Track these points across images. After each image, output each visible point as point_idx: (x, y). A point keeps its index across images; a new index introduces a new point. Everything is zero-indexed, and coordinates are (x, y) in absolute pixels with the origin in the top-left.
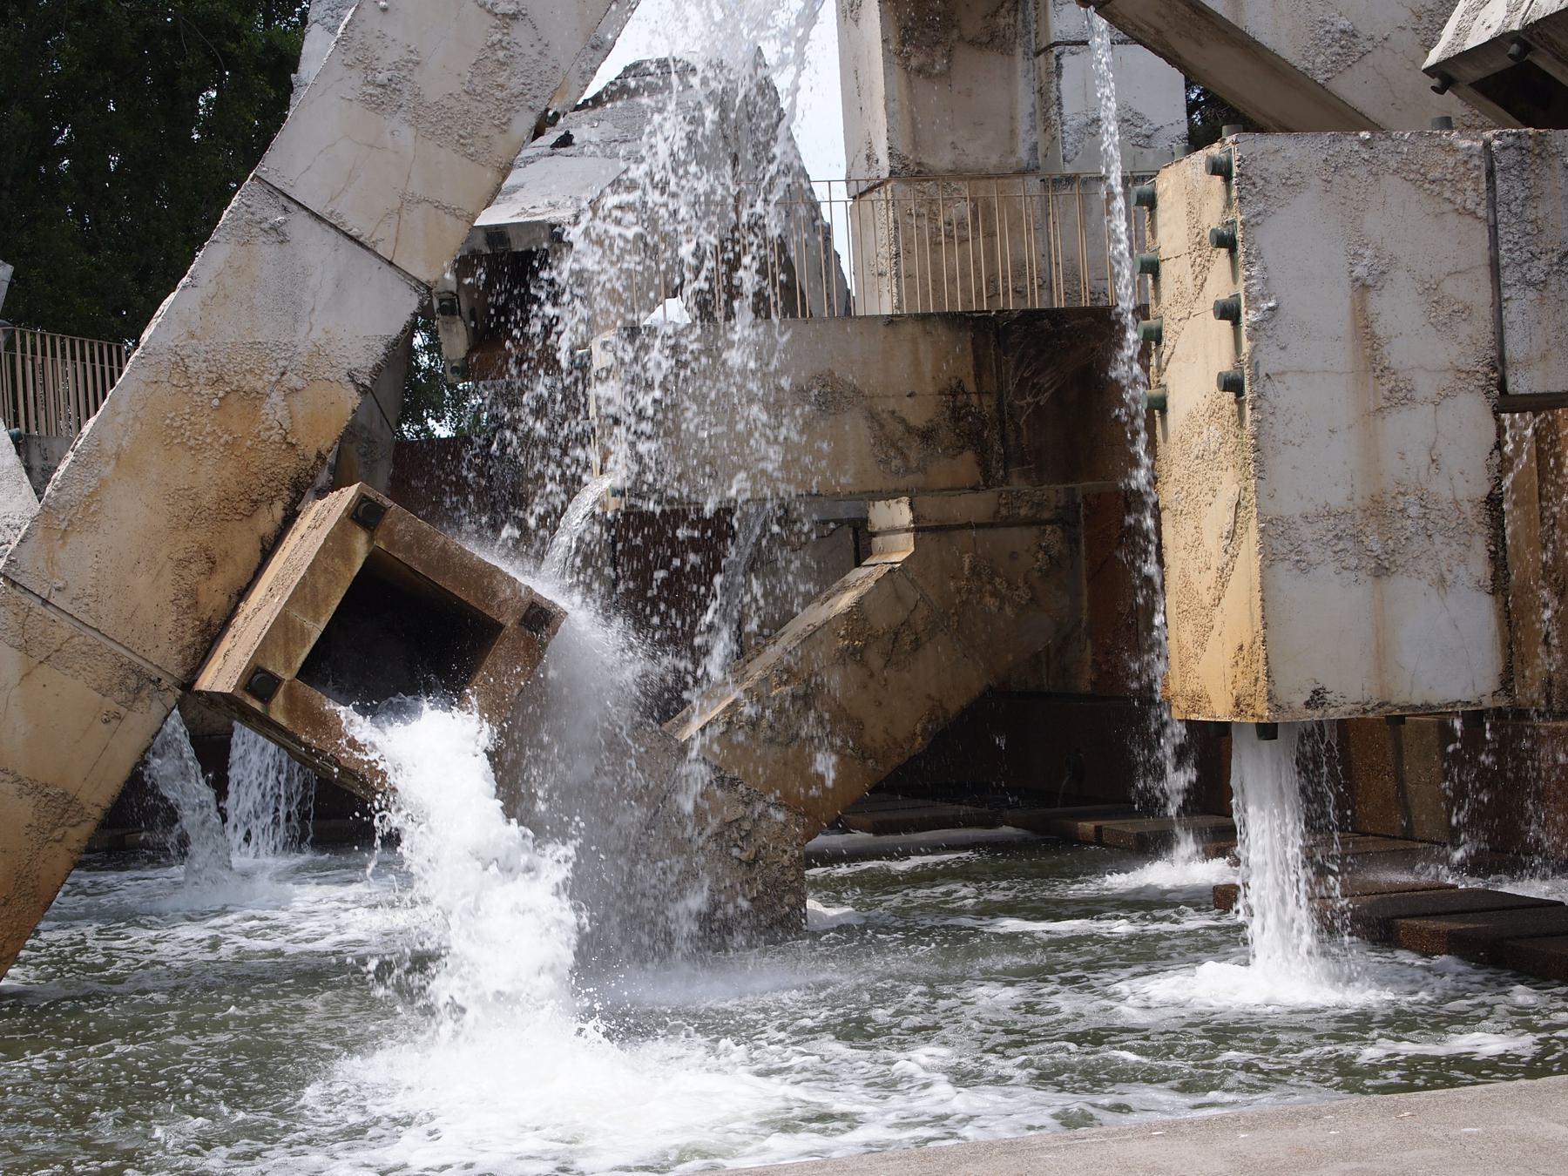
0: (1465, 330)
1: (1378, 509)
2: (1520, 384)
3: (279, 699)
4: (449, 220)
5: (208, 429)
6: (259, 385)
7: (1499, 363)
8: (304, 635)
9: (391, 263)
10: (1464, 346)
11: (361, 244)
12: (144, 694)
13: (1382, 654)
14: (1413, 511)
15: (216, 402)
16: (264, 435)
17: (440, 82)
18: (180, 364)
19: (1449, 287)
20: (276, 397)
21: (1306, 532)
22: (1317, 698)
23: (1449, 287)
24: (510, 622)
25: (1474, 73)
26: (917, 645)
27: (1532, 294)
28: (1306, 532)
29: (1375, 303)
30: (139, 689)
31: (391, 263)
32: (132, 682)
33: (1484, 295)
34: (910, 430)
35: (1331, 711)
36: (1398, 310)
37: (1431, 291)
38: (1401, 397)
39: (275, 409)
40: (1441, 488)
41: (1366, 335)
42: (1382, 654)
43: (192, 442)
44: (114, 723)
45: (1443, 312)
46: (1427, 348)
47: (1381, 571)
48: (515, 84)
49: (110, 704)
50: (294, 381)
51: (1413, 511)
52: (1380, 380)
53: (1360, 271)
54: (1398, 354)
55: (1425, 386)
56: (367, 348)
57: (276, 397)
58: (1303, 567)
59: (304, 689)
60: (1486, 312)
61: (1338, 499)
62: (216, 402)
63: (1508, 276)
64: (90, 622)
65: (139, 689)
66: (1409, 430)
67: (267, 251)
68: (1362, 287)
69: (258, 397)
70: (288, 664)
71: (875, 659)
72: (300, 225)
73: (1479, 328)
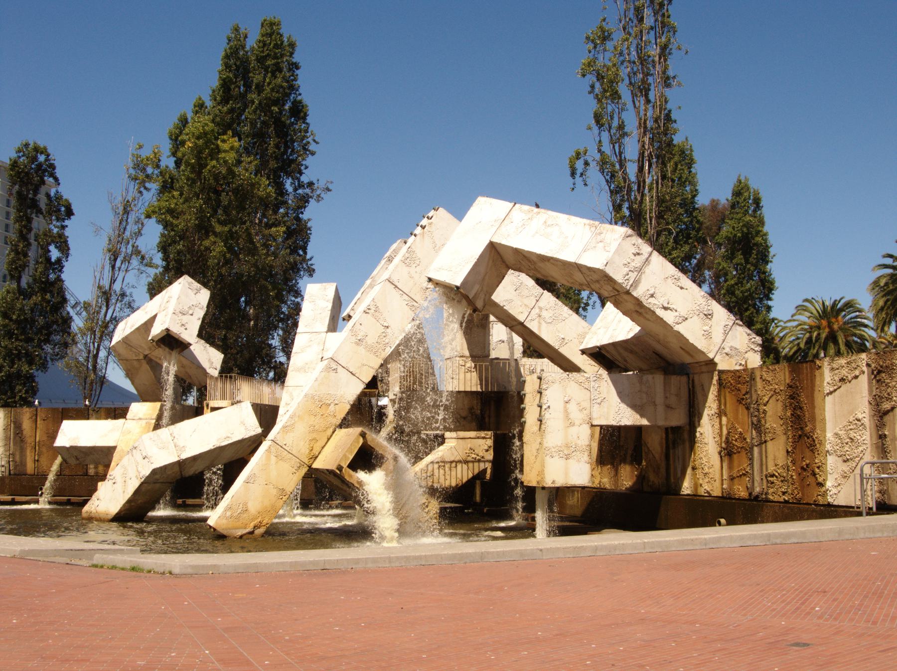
1: (567, 446)
2: (595, 423)
13: (566, 474)
17: (371, 340)
22: (553, 482)
34: (461, 417)
36: (572, 407)
38: (572, 424)
40: (579, 442)
41: (566, 413)
42: (566, 474)
46: (577, 415)
48: (387, 341)
54: (572, 416)
55: (577, 423)
57: (332, 405)
59: (348, 470)
61: (559, 444)
66: (574, 430)
67: (332, 374)
72: (340, 369)
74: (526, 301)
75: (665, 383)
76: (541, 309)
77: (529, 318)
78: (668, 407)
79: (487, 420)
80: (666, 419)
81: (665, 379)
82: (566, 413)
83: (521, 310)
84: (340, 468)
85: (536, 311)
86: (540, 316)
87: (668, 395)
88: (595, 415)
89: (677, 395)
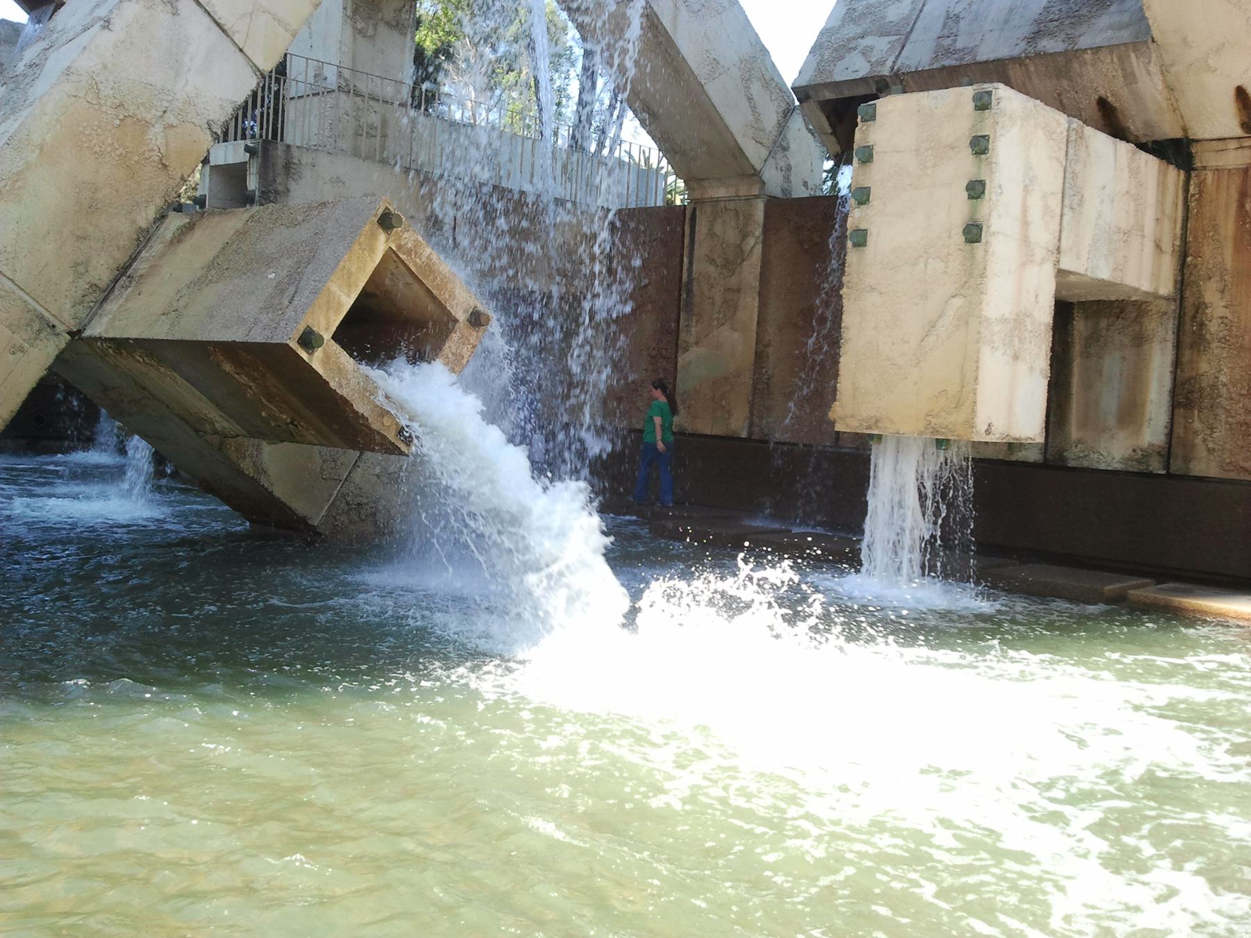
3: (319, 353)
4: (281, 30)
5: (109, 141)
6: (148, 117)
8: (340, 304)
9: (241, 50)
11: (224, 31)
12: (42, 335)
15: (118, 122)
16: (147, 155)
18: (95, 87)
20: (158, 128)
24: (461, 316)
25: (829, 95)
30: (40, 331)
31: (241, 50)
32: (36, 326)
39: (156, 136)
43: (97, 149)
44: (19, 354)
46: (1042, 236)
47: (1016, 358)
49: (18, 339)
50: (174, 122)
56: (222, 107)
57: (158, 128)
62: (118, 122)
64: (8, 274)
65: (40, 331)
67: (162, 15)
69: (147, 124)
84: (309, 340)
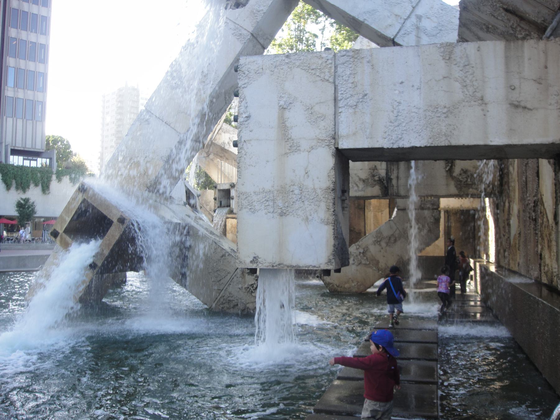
0: (322, 124)
1: (284, 191)
2: (344, 144)
7: (335, 137)
8: (65, 221)
10: (323, 129)
14: (297, 192)
19: (316, 108)
21: (255, 198)
23: (316, 108)
24: (115, 220)
26: (395, 241)
27: (351, 110)
28: (255, 198)
29: (287, 114)
33: (331, 111)
34: (360, 179)
35: (260, 265)
36: (296, 117)
37: (310, 109)
40: (309, 183)
41: (283, 127)
45: (313, 116)
47: (282, 214)
51: (297, 192)
52: (287, 141)
53: (282, 103)
54: (295, 133)
55: (305, 145)
58: (253, 211)
60: (332, 117)
63: (341, 104)
66: (297, 161)
68: (283, 109)
70: (61, 228)
71: (383, 244)
73: (328, 123)
74: (397, 11)
75: (507, 58)
76: (419, 18)
77: (402, 32)
78: (516, 106)
79: (394, 182)
80: (511, 131)
81: (507, 49)
82: (283, 127)
83: (389, 22)
85: (413, 19)
86: (418, 28)
87: (516, 82)
88: (343, 130)
89: (538, 81)
